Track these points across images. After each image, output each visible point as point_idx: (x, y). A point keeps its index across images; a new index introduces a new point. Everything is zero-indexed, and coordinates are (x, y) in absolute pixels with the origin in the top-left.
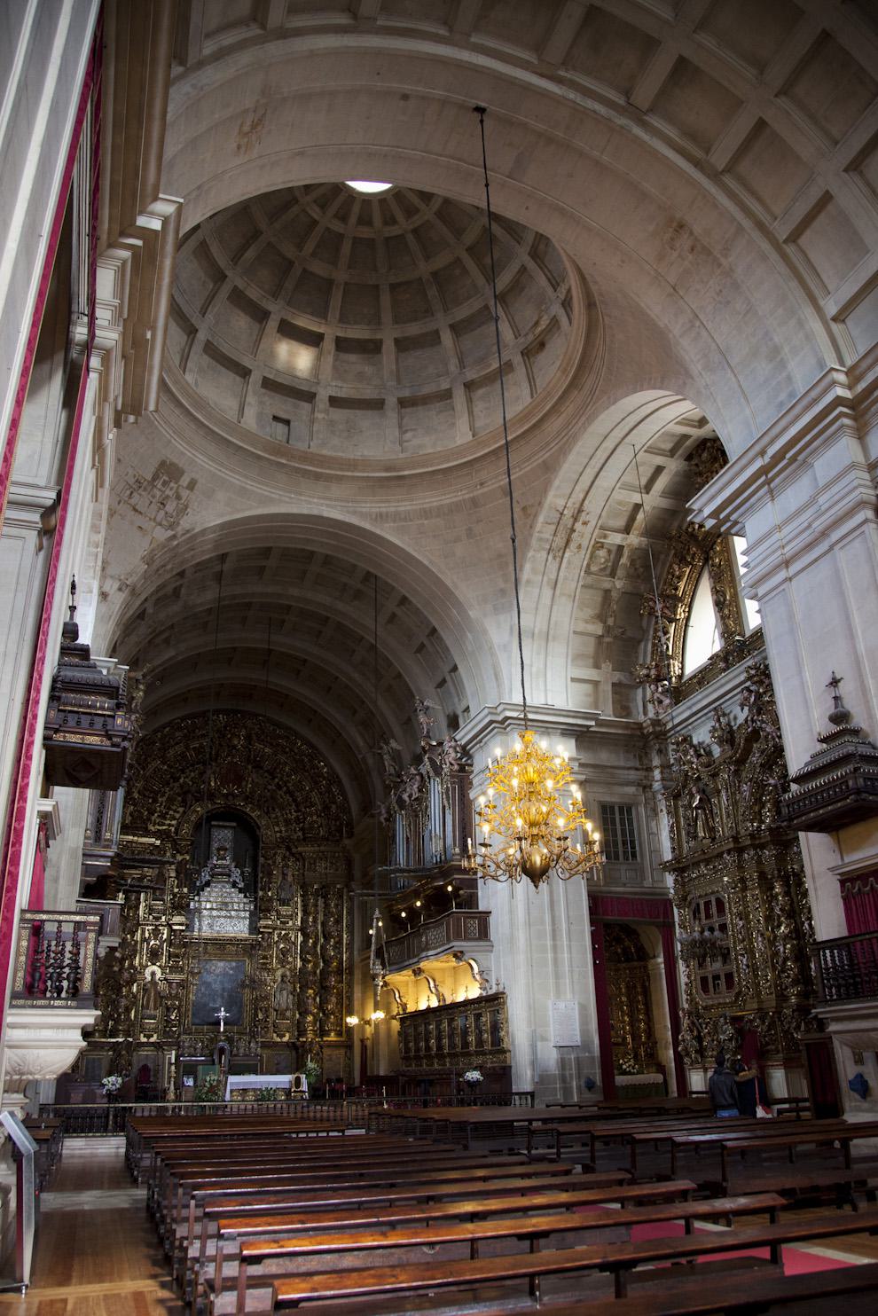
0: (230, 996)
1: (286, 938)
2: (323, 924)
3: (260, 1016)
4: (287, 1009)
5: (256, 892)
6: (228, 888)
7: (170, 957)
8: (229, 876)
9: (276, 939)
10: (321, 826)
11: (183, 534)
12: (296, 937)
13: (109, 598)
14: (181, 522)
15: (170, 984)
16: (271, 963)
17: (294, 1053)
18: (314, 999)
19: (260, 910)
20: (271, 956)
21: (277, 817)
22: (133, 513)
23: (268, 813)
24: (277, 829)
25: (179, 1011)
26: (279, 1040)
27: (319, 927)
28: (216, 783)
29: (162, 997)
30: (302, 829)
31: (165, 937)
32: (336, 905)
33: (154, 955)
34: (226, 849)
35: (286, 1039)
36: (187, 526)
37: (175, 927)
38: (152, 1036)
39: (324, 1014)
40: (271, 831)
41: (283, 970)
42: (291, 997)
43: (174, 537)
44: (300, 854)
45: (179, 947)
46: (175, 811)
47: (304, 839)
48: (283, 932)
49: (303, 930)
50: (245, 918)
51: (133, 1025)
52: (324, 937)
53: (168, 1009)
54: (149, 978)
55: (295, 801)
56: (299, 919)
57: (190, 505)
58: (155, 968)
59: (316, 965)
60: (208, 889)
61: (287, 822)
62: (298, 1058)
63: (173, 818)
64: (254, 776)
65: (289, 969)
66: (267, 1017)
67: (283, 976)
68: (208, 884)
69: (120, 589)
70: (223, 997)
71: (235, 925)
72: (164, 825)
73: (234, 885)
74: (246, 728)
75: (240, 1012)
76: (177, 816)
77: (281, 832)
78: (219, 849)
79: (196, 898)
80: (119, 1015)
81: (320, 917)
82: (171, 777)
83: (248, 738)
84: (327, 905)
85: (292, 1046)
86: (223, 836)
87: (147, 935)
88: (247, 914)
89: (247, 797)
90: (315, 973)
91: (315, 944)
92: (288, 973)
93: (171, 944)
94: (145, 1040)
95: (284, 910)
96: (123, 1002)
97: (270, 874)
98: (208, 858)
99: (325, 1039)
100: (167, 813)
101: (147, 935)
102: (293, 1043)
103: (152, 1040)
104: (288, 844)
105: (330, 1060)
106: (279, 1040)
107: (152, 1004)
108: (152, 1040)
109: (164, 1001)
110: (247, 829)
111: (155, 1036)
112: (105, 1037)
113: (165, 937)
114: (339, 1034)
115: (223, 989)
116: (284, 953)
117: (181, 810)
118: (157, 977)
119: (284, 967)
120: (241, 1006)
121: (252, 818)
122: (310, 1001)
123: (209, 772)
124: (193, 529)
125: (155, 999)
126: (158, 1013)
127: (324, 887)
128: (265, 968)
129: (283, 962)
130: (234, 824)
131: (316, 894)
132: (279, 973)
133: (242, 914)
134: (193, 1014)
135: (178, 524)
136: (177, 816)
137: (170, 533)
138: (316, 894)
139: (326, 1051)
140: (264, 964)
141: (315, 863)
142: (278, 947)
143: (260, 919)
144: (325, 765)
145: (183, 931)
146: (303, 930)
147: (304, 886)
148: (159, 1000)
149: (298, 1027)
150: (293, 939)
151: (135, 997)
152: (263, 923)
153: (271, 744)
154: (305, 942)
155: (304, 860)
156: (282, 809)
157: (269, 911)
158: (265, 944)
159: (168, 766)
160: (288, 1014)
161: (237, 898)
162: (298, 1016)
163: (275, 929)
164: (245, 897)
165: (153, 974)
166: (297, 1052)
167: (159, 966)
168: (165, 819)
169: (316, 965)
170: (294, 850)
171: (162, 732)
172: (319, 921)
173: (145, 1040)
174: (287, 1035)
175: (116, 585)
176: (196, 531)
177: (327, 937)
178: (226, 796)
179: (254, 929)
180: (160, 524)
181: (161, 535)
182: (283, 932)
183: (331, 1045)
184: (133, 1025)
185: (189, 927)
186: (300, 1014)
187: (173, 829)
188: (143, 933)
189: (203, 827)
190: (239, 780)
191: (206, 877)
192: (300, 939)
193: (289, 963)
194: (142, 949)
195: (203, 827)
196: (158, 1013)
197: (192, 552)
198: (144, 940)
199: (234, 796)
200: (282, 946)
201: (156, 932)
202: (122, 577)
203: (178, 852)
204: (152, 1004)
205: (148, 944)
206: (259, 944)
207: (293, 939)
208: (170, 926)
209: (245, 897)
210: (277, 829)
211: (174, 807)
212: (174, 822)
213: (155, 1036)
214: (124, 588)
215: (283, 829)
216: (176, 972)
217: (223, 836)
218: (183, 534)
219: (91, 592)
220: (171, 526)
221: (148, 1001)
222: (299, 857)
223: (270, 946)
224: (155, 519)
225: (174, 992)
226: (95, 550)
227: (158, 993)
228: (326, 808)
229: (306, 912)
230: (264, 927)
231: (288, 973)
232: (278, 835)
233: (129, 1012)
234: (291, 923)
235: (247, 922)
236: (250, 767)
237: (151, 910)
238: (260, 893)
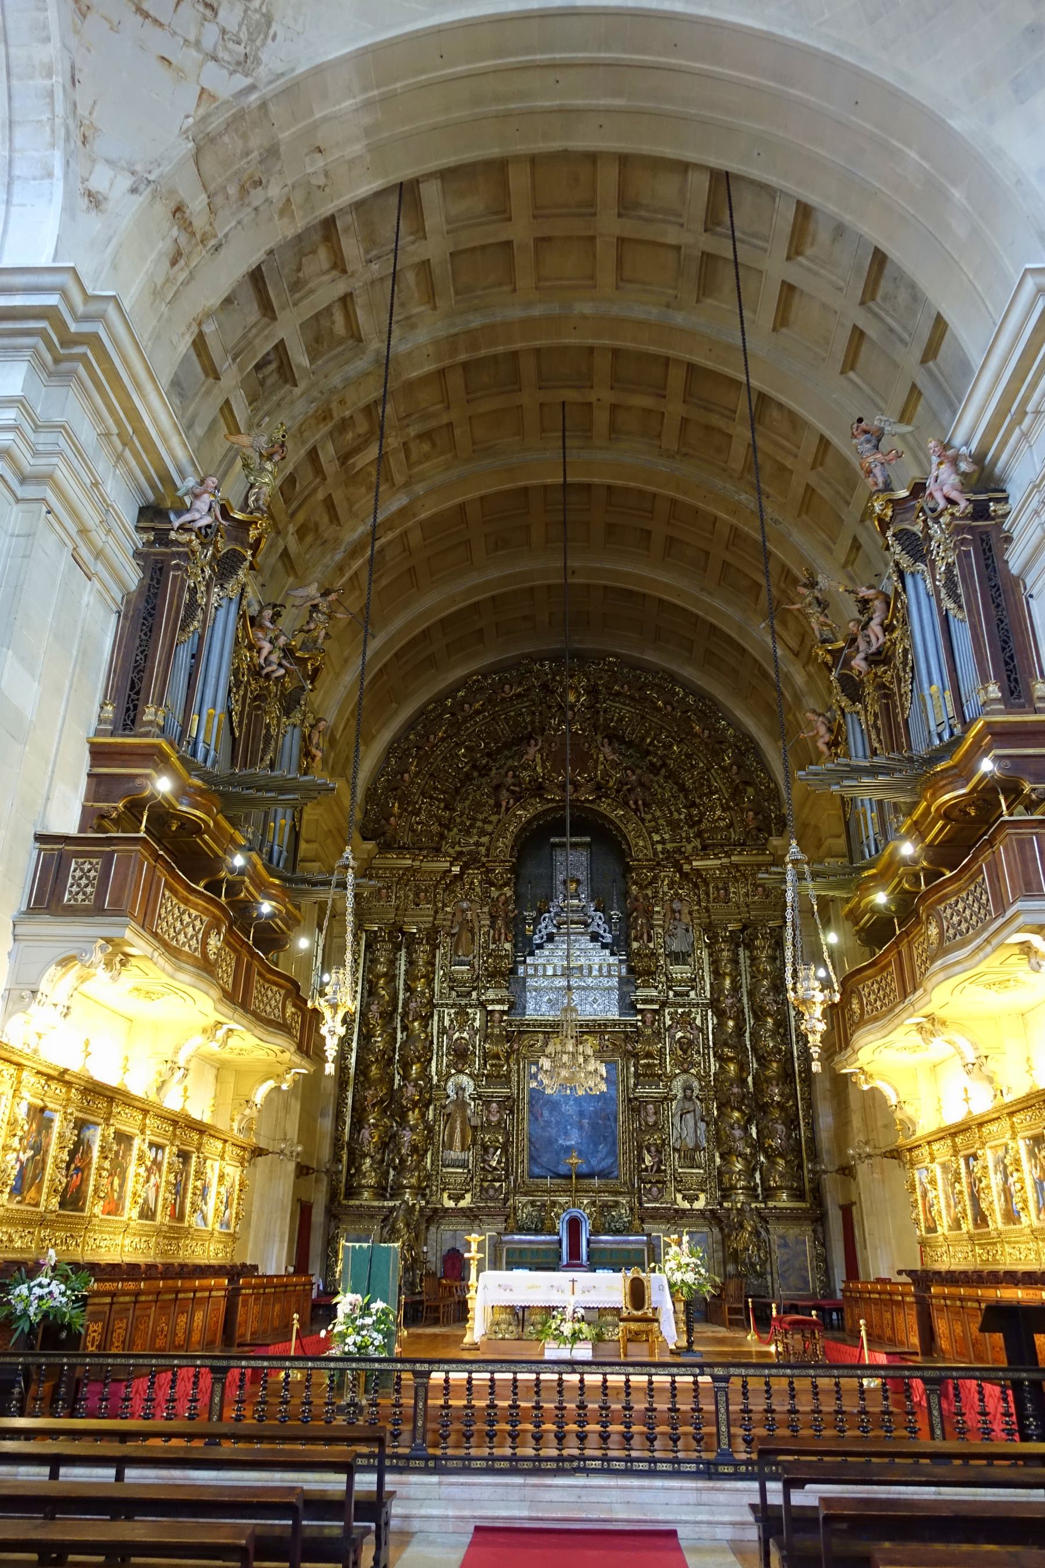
0: (594, 1126)
1: (685, 1021)
2: (751, 994)
3: (648, 1160)
4: (697, 1148)
5: (629, 945)
6: (585, 942)
7: (486, 1056)
8: (587, 925)
9: (668, 1022)
10: (731, 825)
11: (271, 82)
12: (704, 1018)
13: (109, 206)
14: (264, 56)
15: (487, 1104)
16: (662, 1064)
17: (716, 1230)
18: (746, 1130)
19: (638, 971)
20: (661, 1053)
21: (655, 819)
22: (139, 19)
23: (636, 810)
24: (656, 838)
25: (505, 1148)
26: (686, 1205)
27: (745, 1000)
28: (544, 767)
29: (475, 1128)
30: (699, 835)
31: (477, 1024)
32: (773, 959)
33: (461, 1055)
34: (578, 882)
35: (700, 1204)
36: (280, 68)
37: (490, 1008)
38: (462, 1197)
39: (767, 1157)
40: (641, 845)
41: (685, 1076)
42: (702, 1125)
43: (253, 88)
44: (698, 872)
45: (499, 1040)
46: (485, 821)
47: (704, 848)
48: (680, 1011)
49: (714, 1004)
50: (610, 988)
51: (428, 1177)
52: (757, 1018)
53: (485, 1149)
54: (453, 1096)
55: (682, 788)
56: (708, 987)
57: (277, 16)
58: (464, 1080)
59: (743, 1067)
60: (550, 946)
61: (674, 825)
62: (723, 1239)
63: (482, 833)
64: (607, 750)
65: (697, 1076)
66: (660, 1162)
67: (687, 1088)
68: (551, 938)
69: (134, 190)
70: (581, 1128)
71: (595, 1001)
72: (468, 844)
73: (595, 937)
74: (587, 675)
75: (612, 1153)
76: (489, 828)
77: (663, 842)
78: (565, 882)
79: (529, 960)
80: (402, 1161)
81: (745, 980)
82: (474, 767)
83: (592, 691)
84: (753, 959)
85: (711, 1217)
86: (572, 862)
87: (447, 1023)
88: (615, 982)
89: (599, 787)
90: (743, 1082)
91: (739, 1030)
92: (696, 1084)
93: (486, 1038)
94: (451, 1204)
95: (680, 972)
96: (407, 1136)
97: (649, 914)
98: (550, 898)
99: (771, 1204)
100: (472, 826)
101: (447, 1023)
102: (711, 1211)
103: (463, 1204)
104: (675, 859)
105: (786, 1245)
106: (686, 1205)
107: (457, 1143)
108: (463, 1204)
109: (480, 1135)
110: (606, 840)
111: (468, 1196)
112: (382, 1197)
113: (477, 1024)
114: (798, 1194)
115: (581, 1114)
116: (686, 1046)
117: (494, 818)
118: (467, 1094)
119: (685, 1071)
120: (614, 1143)
121: (612, 822)
122: (738, 1133)
123: (532, 750)
124: (293, 70)
125: (463, 1131)
126: (470, 1156)
127: (745, 927)
128: (648, 1076)
129: (685, 1065)
130: (588, 839)
131: (734, 940)
132: (677, 1085)
133: (606, 982)
134: (532, 1159)
135: (258, 61)
136: (489, 828)
137: (241, 81)
138: (734, 940)
139: (776, 1231)
140: (648, 1065)
141: (726, 890)
142: (673, 1037)
143: (637, 988)
144: (729, 724)
145: (503, 1012)
146: (714, 1004)
147: (709, 928)
148: (470, 1132)
149: (721, 1182)
150: (698, 1022)
151: (430, 1129)
152: (641, 993)
153: (632, 698)
154: (720, 1027)
155: (706, 883)
156: (662, 803)
157: (651, 973)
158: (648, 1031)
159: (467, 748)
160: (701, 1157)
161: (599, 958)
162: (718, 1160)
163: (664, 1004)
164: (612, 954)
165: (460, 1089)
166: (722, 1230)
167: (470, 1075)
168: (468, 833)
169: (743, 1067)
170: (686, 868)
171: (454, 698)
172: (744, 990)
173: (451, 1204)
174: (702, 1196)
175: (125, 182)
176: (299, 71)
177: (759, 1014)
178: (563, 787)
179: (628, 1006)
180: (215, 59)
181: (225, 84)
182: (680, 1011)
183: (782, 1216)
184: (428, 1177)
185: (515, 1006)
186: (722, 1157)
187: (483, 850)
188: (441, 1019)
189: (535, 842)
190: (582, 759)
191: (546, 926)
192: (712, 1021)
193: (693, 1064)
194: (440, 1046)
195: (535, 842)
196: (470, 1156)
197: (320, 162)
198: (443, 1031)
199: (576, 786)
200: (680, 1034)
201: (462, 1012)
202: (138, 168)
203: (492, 884)
204: (457, 1143)
205: (450, 1038)
206: (639, 1032)
207: (698, 1022)
208: (482, 1005)
209: (612, 954)
210: (656, 838)
211: (481, 817)
212: (485, 840)
213: (468, 1196)
214: (142, 187)
215: (666, 836)
216: (495, 1085)
217: (572, 862)
218: (271, 82)
219: (50, 175)
220: (245, 64)
221: (451, 1136)
222: (696, 880)
223: (657, 1034)
224: (198, 44)
225: (494, 1119)
226: (47, 82)
227: (465, 1120)
228: (737, 793)
229: (717, 974)
230: (645, 1001)
231: (696, 1084)
232: (659, 847)
233: (423, 1156)
234: (692, 994)
235: (615, 995)
236: (599, 738)
237: (452, 981)
238: (635, 945)
